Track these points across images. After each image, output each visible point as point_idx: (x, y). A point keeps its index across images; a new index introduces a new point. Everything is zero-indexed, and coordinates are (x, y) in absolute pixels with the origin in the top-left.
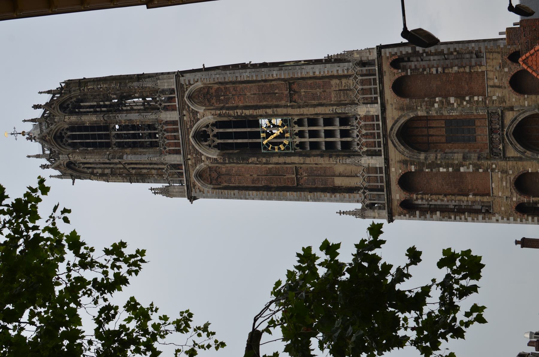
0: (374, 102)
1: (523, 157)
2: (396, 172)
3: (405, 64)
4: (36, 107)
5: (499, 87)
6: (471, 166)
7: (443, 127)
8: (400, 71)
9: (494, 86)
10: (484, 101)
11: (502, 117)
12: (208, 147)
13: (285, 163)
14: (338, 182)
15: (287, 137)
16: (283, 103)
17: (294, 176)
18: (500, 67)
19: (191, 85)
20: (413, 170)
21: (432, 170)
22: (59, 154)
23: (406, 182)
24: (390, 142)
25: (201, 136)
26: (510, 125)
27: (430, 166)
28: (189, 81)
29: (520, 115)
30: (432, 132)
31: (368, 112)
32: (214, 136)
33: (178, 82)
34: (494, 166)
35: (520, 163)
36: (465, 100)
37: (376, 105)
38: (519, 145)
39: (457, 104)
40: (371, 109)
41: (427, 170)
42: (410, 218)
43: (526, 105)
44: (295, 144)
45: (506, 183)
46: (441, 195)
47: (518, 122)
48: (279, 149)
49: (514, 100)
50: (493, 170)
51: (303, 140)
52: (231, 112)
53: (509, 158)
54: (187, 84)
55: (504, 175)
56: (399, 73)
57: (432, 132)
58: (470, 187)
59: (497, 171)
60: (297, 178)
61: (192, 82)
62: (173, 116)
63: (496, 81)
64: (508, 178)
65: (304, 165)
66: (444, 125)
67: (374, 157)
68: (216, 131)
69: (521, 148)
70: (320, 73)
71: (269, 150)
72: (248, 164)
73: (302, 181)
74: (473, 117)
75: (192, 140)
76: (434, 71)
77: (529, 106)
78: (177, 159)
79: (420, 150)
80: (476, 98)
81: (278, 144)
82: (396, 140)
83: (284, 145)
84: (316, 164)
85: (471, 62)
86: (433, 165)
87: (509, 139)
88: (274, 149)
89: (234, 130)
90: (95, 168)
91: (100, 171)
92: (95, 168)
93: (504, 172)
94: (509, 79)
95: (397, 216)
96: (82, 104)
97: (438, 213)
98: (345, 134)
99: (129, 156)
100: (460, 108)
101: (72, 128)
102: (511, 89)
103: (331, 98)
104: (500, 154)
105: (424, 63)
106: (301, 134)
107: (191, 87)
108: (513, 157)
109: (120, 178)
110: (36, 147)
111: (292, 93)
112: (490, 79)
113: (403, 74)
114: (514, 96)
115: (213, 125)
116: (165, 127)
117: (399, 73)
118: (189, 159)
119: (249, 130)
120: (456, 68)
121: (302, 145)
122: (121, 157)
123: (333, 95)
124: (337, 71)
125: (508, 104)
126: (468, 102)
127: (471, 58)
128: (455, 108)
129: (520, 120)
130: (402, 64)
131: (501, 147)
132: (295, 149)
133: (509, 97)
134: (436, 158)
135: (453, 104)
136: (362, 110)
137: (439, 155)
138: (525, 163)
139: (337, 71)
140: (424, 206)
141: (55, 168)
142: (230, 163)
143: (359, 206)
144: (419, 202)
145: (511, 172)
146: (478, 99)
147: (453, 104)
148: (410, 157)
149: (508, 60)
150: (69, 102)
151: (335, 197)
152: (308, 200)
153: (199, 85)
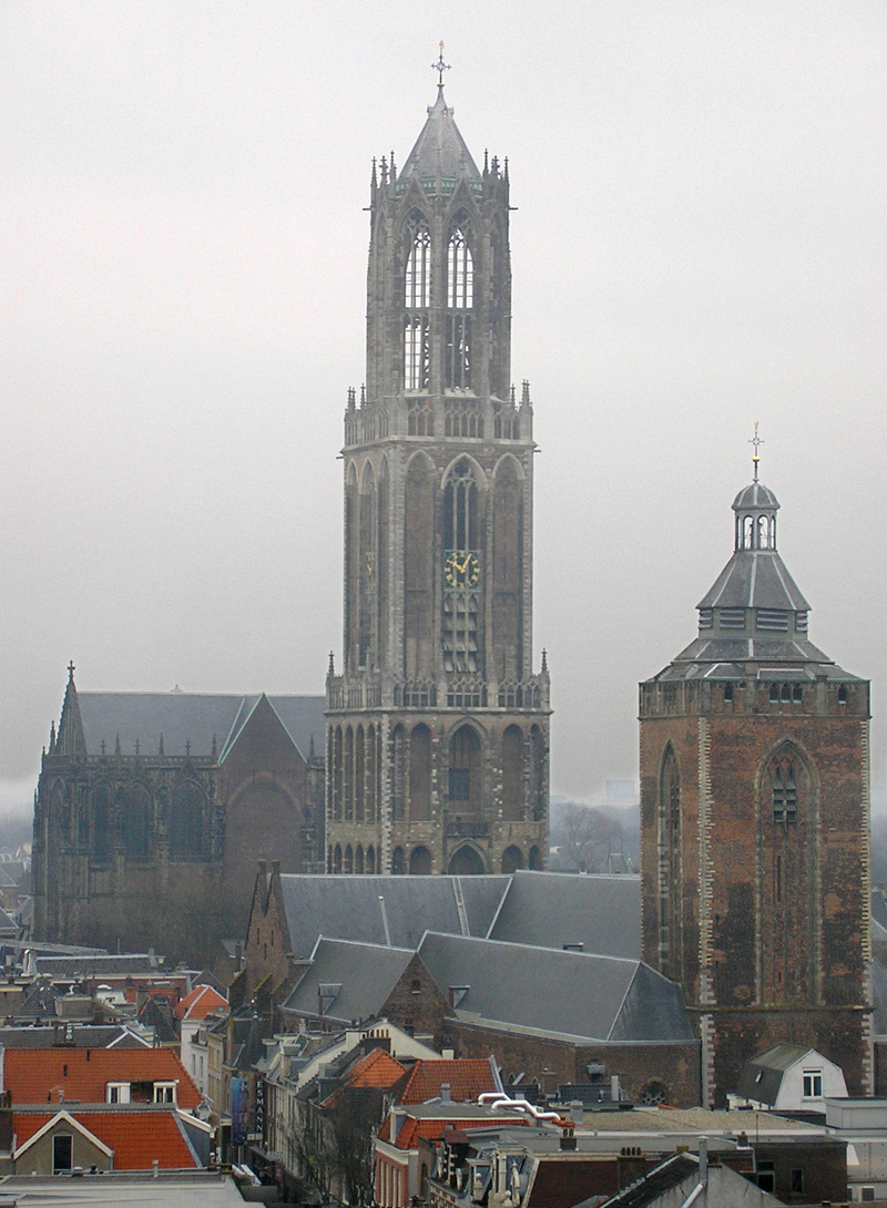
2: (432, 721)
10: (498, 819)
13: (434, 583)
19: (523, 463)
22: (443, 215)
23: (422, 730)
25: (462, 468)
28: (526, 463)
50: (435, 825)
54: (525, 459)
56: (527, 733)
61: (526, 466)
68: (468, 487)
75: (462, 455)
80: (501, 811)
82: (463, 723)
83: (452, 581)
93: (433, 835)
94: (517, 845)
98: (461, 654)
107: (520, 464)
115: (474, 484)
116: (477, 417)
117: (527, 733)
119: (467, 534)
125: (494, 843)
136: (493, 688)
142: (435, 506)
153: (522, 477)
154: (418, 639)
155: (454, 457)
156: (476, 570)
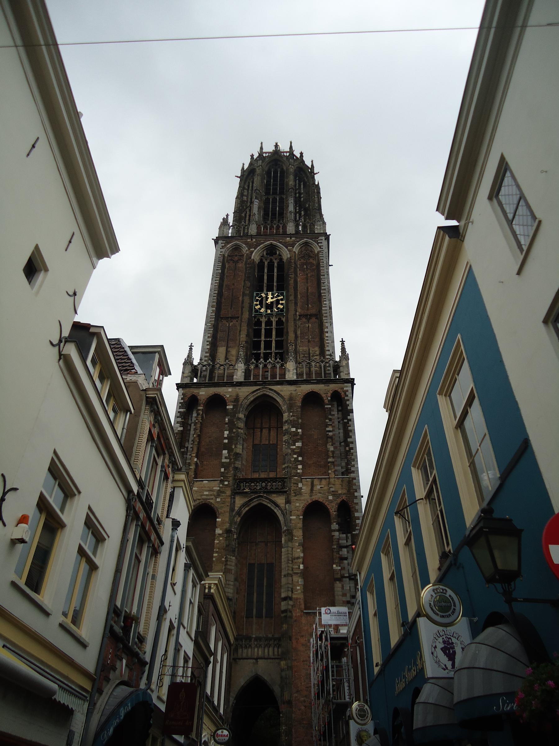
0: (299, 375)
1: (234, 513)
3: (336, 406)
4: (301, 154)
5: (312, 490)
6: (228, 460)
7: (269, 442)
8: (329, 398)
9: (313, 485)
10: (297, 474)
11: (280, 492)
12: (261, 255)
13: (242, 308)
14: (221, 351)
15: (267, 311)
16: (299, 310)
17: (230, 316)
18: (333, 491)
19: (318, 244)
20: (228, 407)
21: (226, 424)
23: (217, 402)
24: (259, 387)
25: (271, 250)
26: (270, 500)
27: (231, 422)
28: (321, 243)
29: (282, 511)
30: (265, 432)
31: (289, 371)
32: (271, 260)
33: (320, 234)
34: (226, 483)
35: (227, 509)
36: (298, 457)
37: (295, 377)
38: (247, 509)
39: (295, 449)
40: (291, 373)
41: (227, 419)
42: (179, 403)
43: (291, 517)
44: (260, 318)
45: (206, 495)
46: (200, 431)
47: (273, 508)
48: (257, 305)
49: (298, 504)
51: (263, 325)
52: (293, 270)
53: (234, 498)
55: (215, 493)
56: (327, 398)
57: (265, 432)
58: (205, 463)
59: (221, 486)
60: (228, 317)
61: (319, 244)
62: (291, 228)
63: (319, 487)
64: (213, 497)
65: (239, 321)
66: (271, 443)
67: (244, 374)
69: (245, 510)
70: (327, 337)
71: (255, 297)
72: (244, 281)
73: (224, 322)
74: (278, 470)
76: (330, 428)
77: (291, 519)
78: (253, 229)
79: (247, 417)
80: (300, 467)
81: (261, 304)
82: (260, 393)
83: (260, 309)
84: (240, 332)
85: (338, 465)
86: (232, 426)
87: (254, 498)
88: (257, 300)
89: (275, 274)
90: (248, 190)
91: (246, 193)
92: (248, 190)
93: (220, 493)
95: (183, 392)
96: (302, 183)
97: (181, 429)
99: (257, 203)
100: (290, 451)
101: (282, 172)
102: (310, 502)
103: (302, 347)
104: (239, 490)
105: (336, 423)
106: (269, 323)
108: (234, 502)
109: (239, 205)
110: (269, 148)
111: (308, 317)
112: (320, 482)
113: (326, 401)
114: (302, 505)
115: (281, 260)
117: (327, 398)
118: (252, 240)
120: (332, 449)
121: (259, 323)
122: (256, 198)
123: (305, 348)
124: (329, 350)
125: (293, 498)
126: (296, 459)
127: (342, 468)
128: (291, 448)
129: (275, 511)
130: (335, 403)
131: (247, 490)
132: (255, 317)
133: (300, 500)
134: (239, 428)
135: (295, 445)
137: (242, 431)
138: (228, 514)
139: (329, 350)
140: (190, 420)
141: (251, 164)
142: (246, 268)
143: (196, 362)
144: (195, 415)
145: (218, 500)
146: (299, 469)
147: (295, 445)
148: (241, 404)
149: (341, 500)
150: (304, 175)
151: (207, 345)
152: (206, 324)
154: (227, 347)
155: (263, 243)
156: (281, 302)
